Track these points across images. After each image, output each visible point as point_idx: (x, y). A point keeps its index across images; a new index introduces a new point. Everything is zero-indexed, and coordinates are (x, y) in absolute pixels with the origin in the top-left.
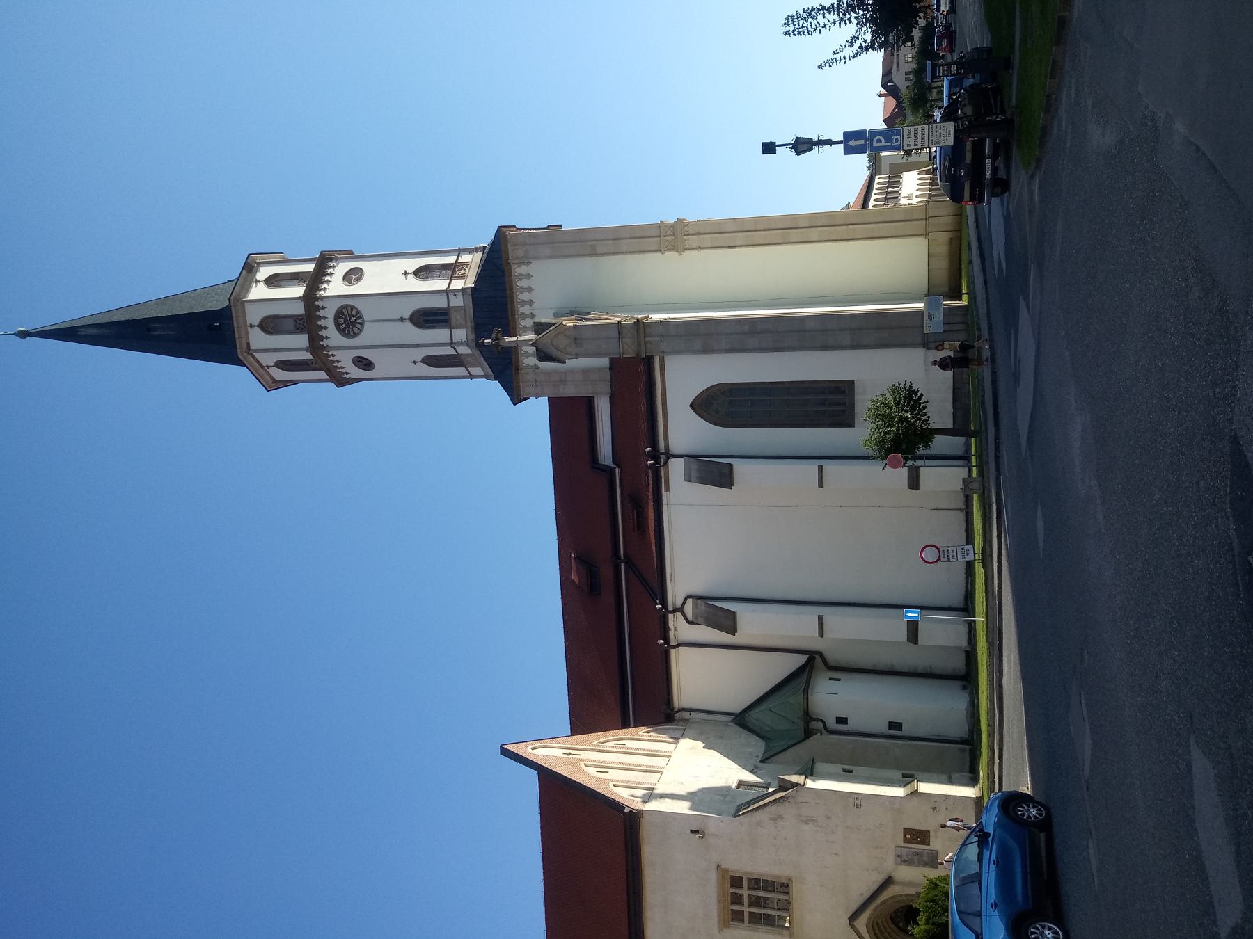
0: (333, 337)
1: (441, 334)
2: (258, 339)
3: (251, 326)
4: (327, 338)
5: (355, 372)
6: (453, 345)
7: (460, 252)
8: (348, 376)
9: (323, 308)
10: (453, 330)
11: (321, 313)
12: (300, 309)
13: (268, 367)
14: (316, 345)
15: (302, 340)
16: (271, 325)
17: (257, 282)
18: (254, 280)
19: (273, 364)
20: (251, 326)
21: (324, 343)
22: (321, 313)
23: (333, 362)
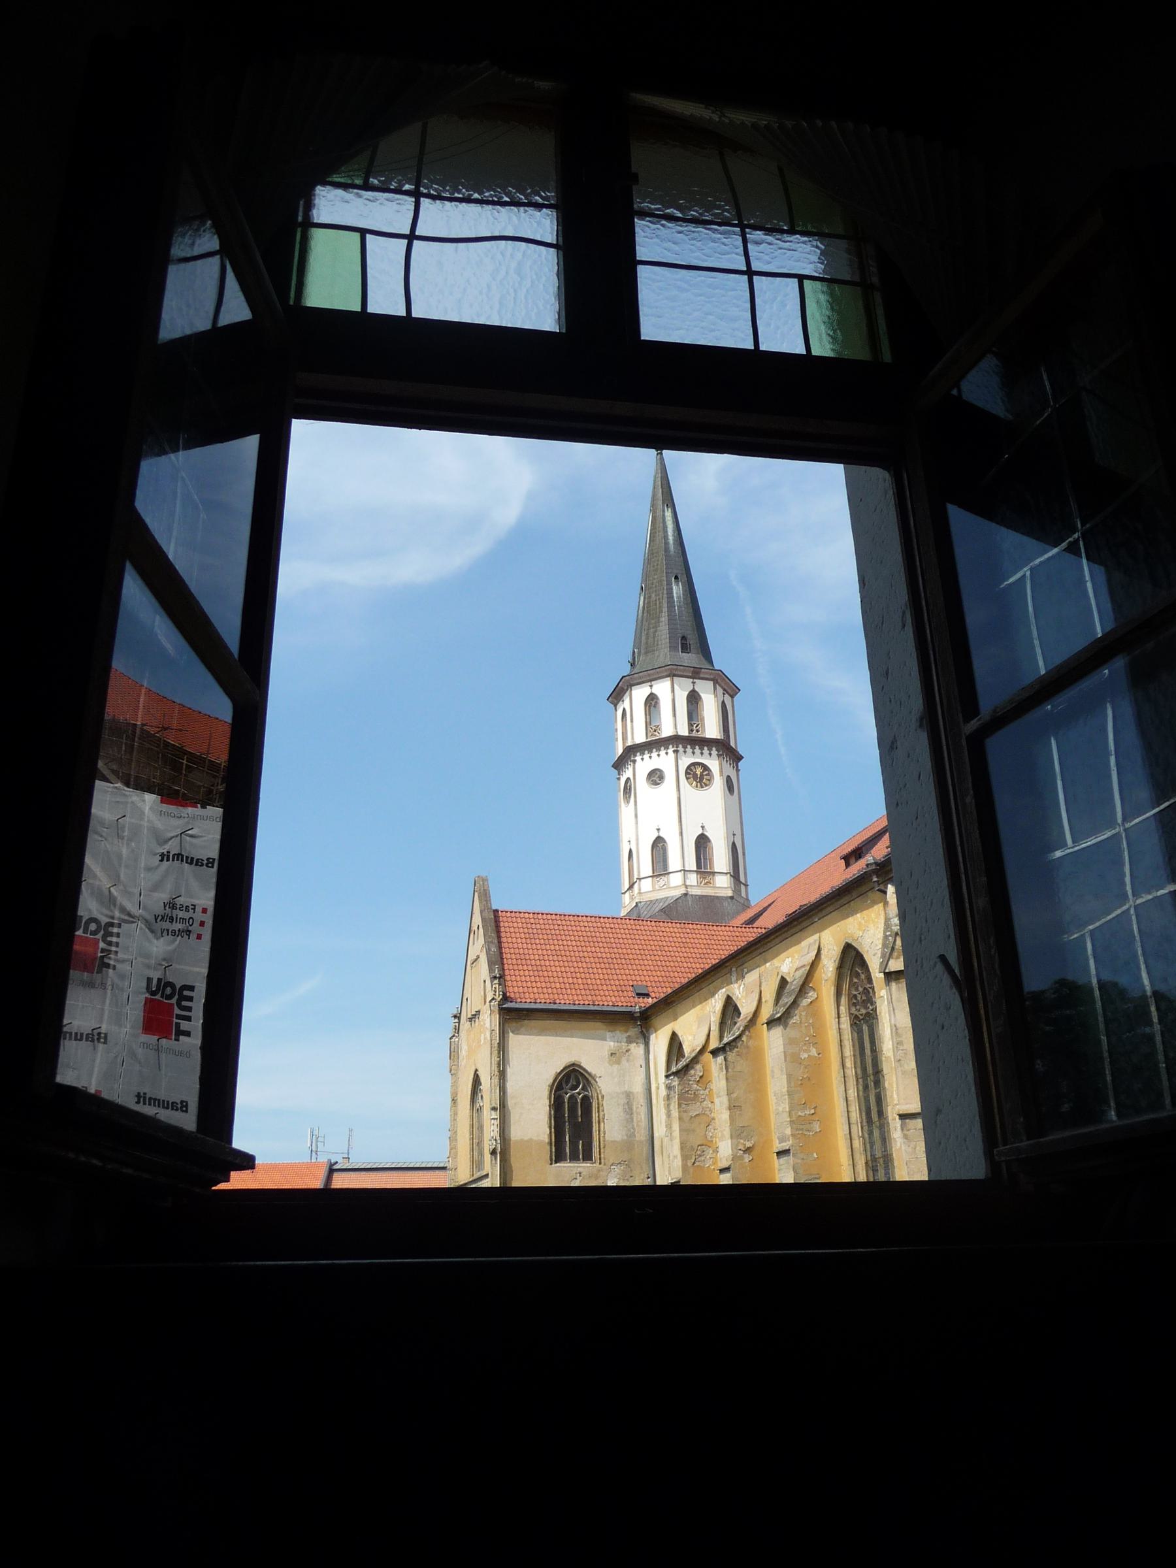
1: (692, 864)
3: (694, 683)
4: (685, 752)
6: (683, 872)
7: (746, 885)
10: (695, 875)
11: (706, 751)
13: (651, 686)
14: (675, 740)
15: (684, 731)
16: (694, 699)
17: (724, 694)
19: (654, 691)
22: (706, 751)
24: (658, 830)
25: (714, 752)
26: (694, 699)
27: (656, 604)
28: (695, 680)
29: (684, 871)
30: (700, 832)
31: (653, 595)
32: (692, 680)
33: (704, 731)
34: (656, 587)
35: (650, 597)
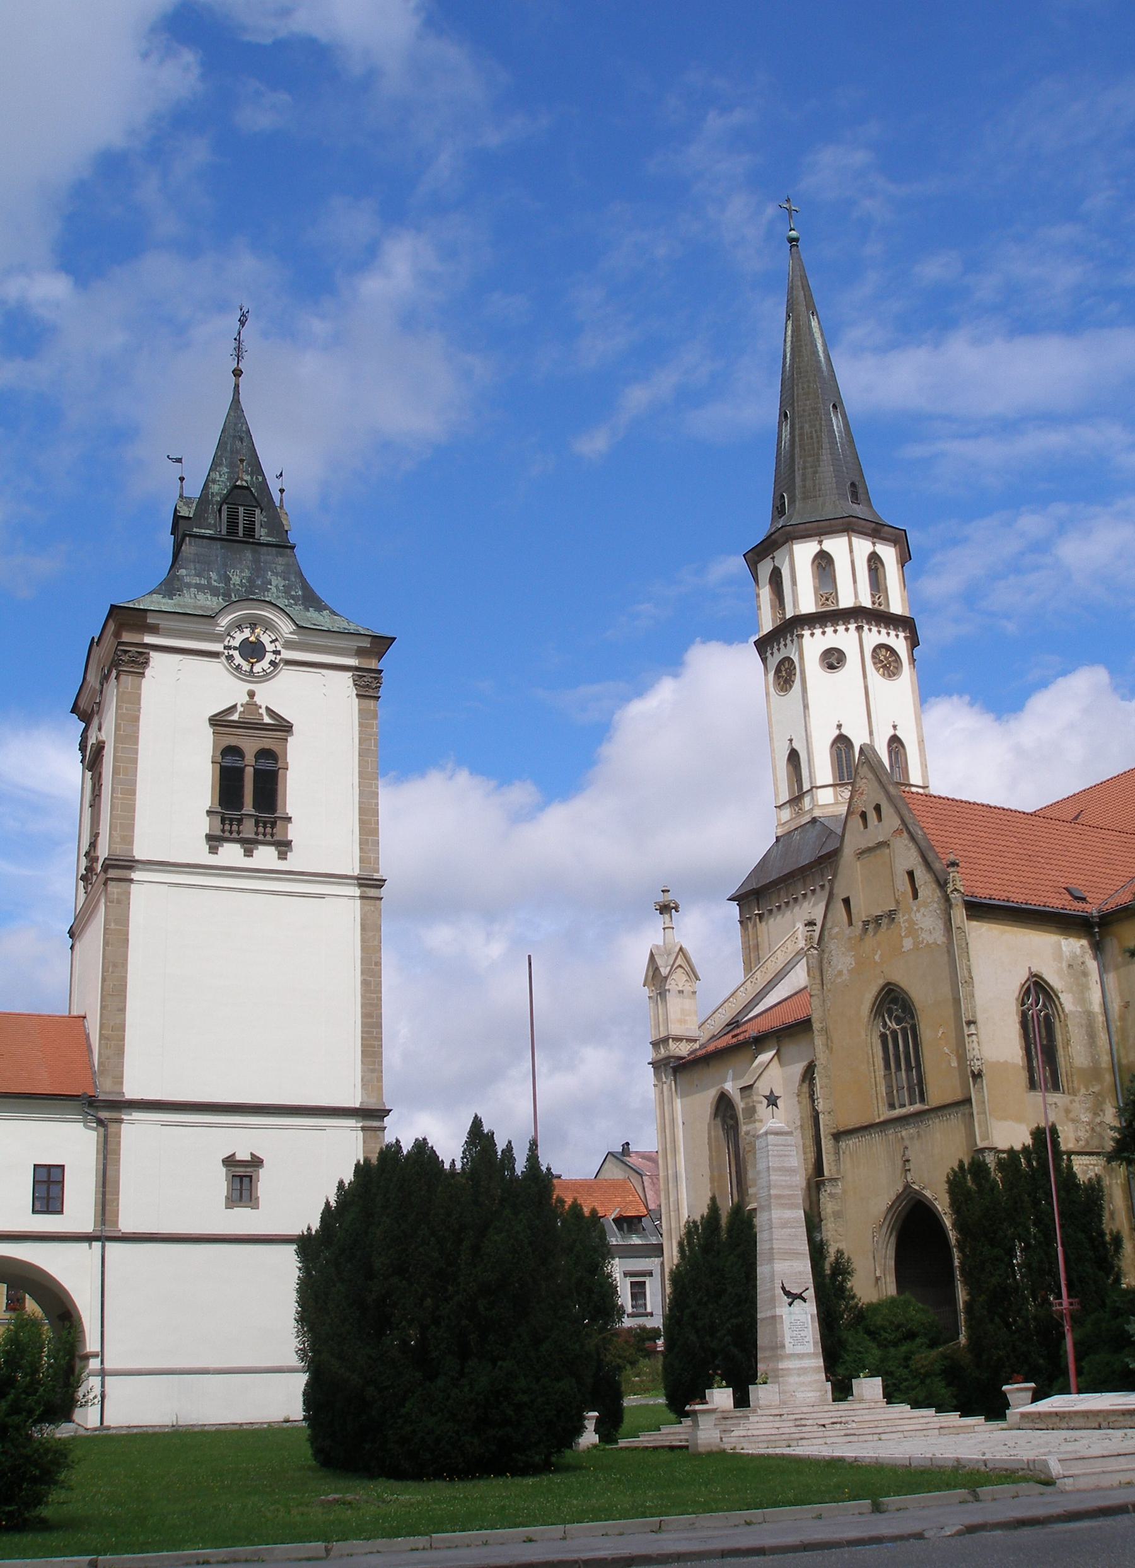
0: (814, 643)
2: (804, 552)
3: (820, 542)
5: (773, 662)
8: (768, 654)
9: (847, 630)
10: (831, 789)
12: (846, 601)
13: (773, 558)
15: (807, 605)
16: (824, 561)
17: (874, 543)
18: (875, 540)
20: (820, 542)
21: (806, 633)
23: (785, 640)
24: (791, 740)
25: (852, 627)
26: (824, 561)
27: (812, 438)
28: (822, 537)
29: (818, 788)
30: (837, 732)
31: (807, 426)
32: (818, 538)
33: (838, 605)
34: (809, 415)
35: (802, 428)
